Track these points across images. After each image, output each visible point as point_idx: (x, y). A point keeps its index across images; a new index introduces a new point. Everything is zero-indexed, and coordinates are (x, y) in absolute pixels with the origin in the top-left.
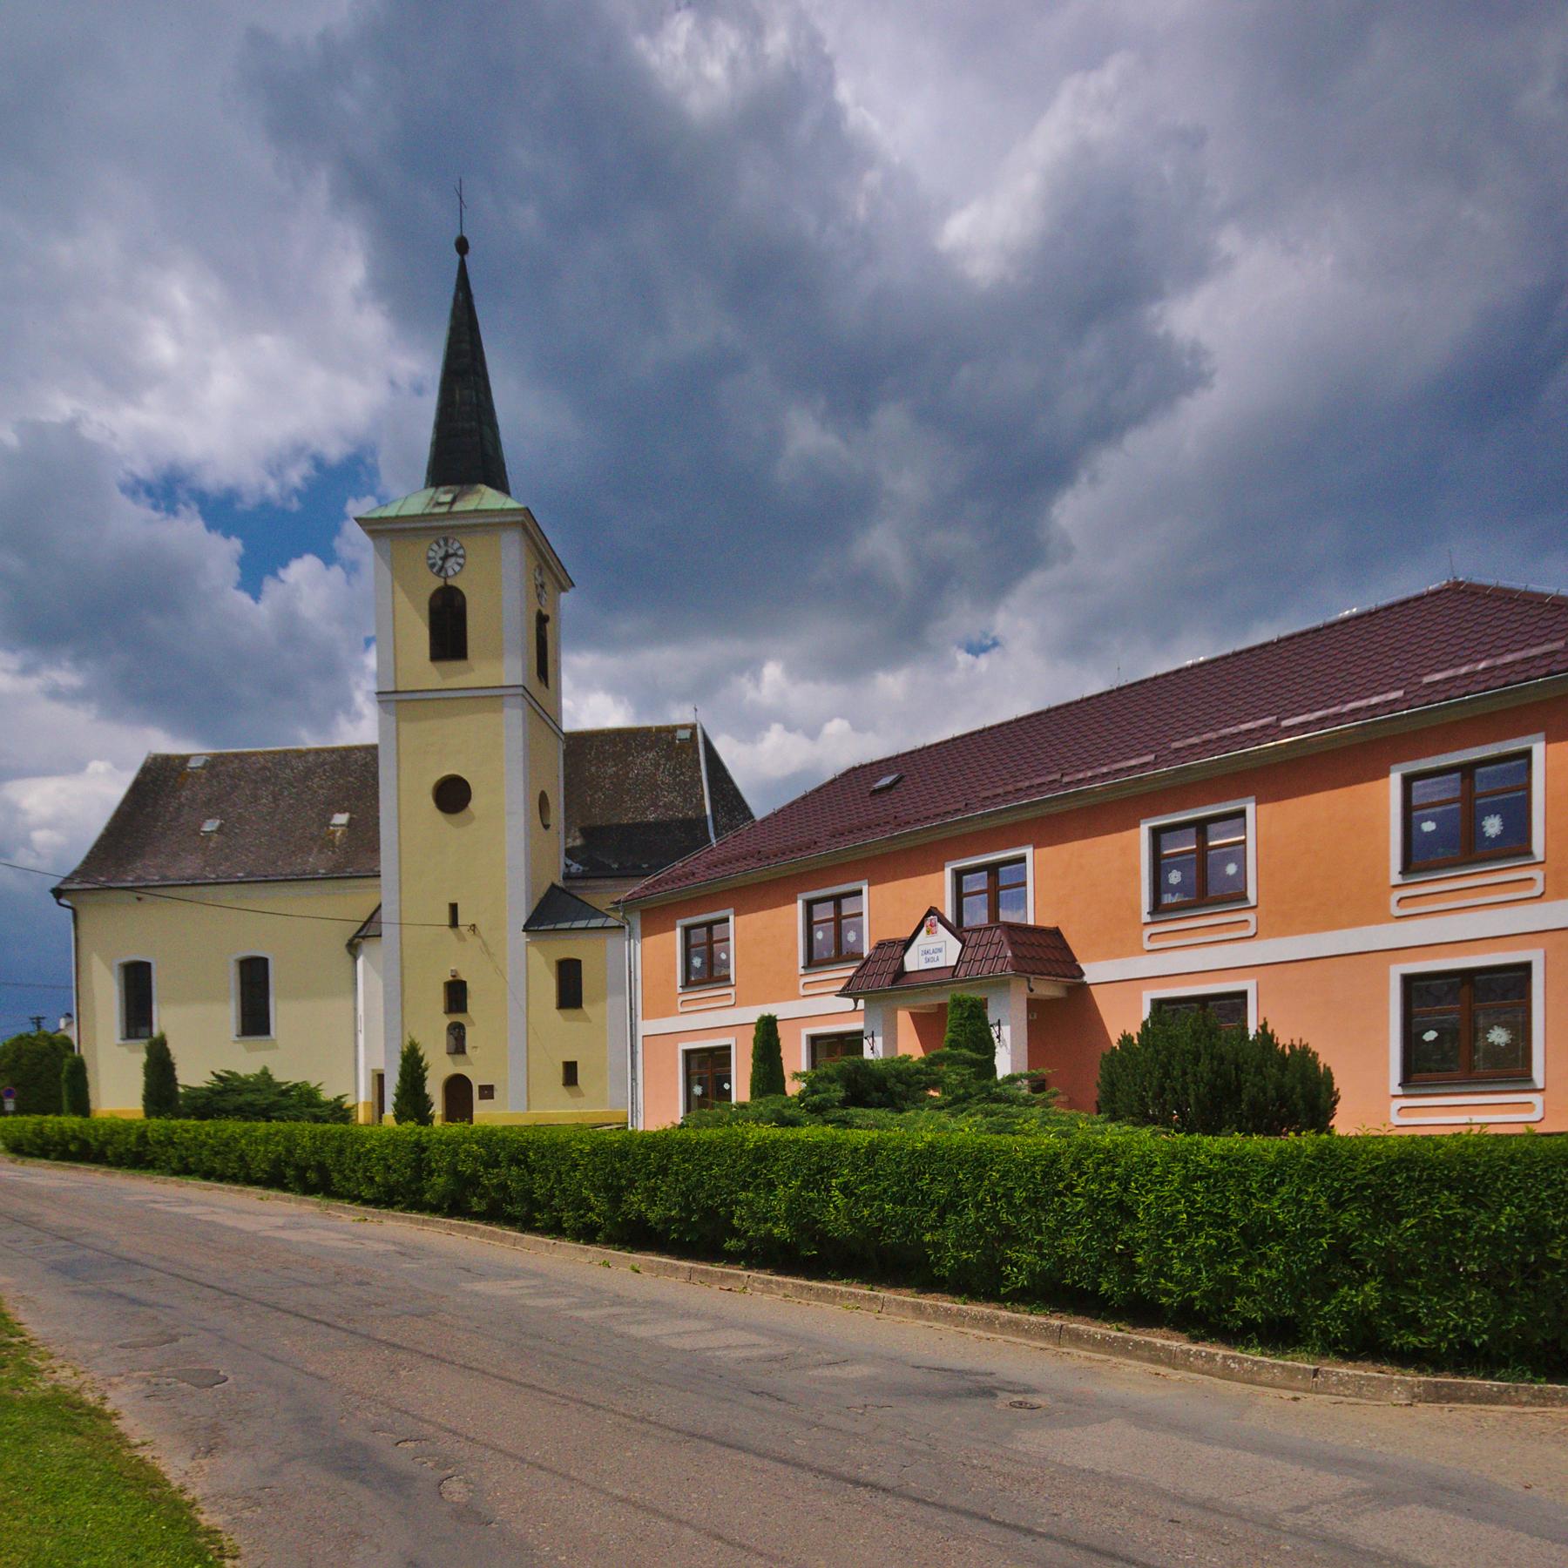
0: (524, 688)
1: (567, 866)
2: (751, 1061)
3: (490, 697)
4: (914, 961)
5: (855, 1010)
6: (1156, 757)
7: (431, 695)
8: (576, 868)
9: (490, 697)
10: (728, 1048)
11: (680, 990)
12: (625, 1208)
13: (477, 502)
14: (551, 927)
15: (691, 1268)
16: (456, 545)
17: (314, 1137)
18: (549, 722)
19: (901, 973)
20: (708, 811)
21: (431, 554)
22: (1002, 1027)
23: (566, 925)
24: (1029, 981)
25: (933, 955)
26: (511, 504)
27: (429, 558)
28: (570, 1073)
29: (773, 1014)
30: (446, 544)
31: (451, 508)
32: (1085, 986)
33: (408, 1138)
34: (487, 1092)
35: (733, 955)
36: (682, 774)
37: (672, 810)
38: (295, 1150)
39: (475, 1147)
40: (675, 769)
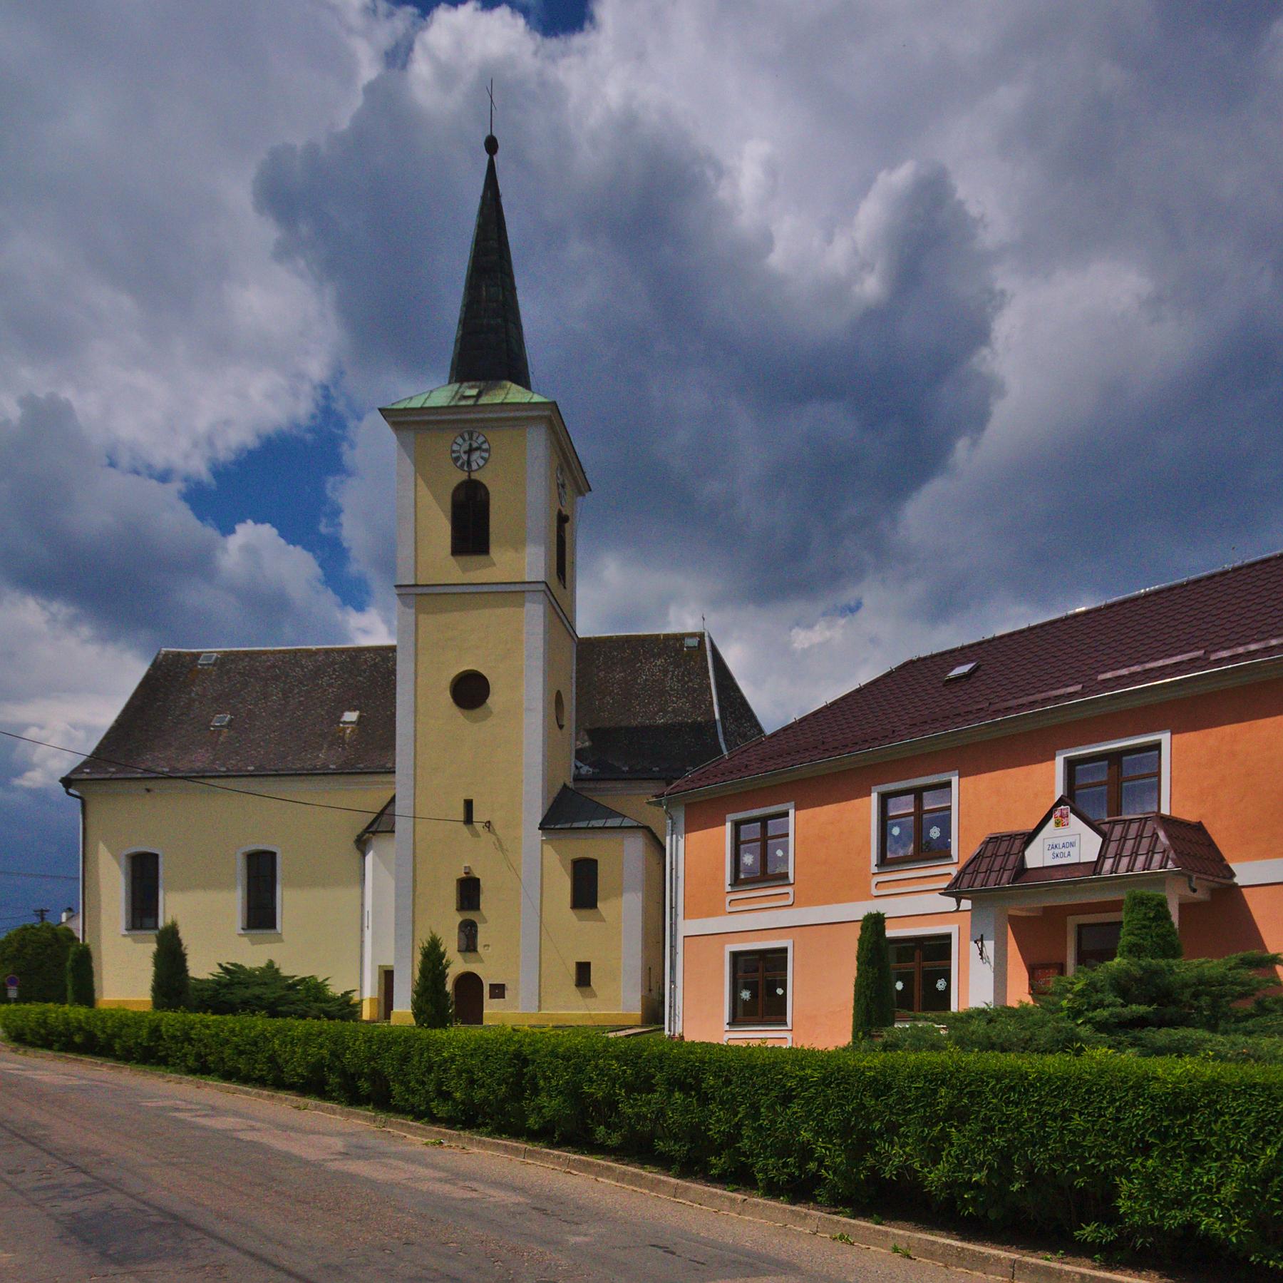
0: (546, 583)
1: (577, 767)
2: (856, 963)
3: (512, 593)
4: (1036, 856)
5: (957, 911)
6: (1083, 687)
7: (454, 590)
8: (585, 770)
9: (512, 593)
10: (785, 950)
11: (728, 889)
12: (870, 1160)
13: (504, 396)
14: (567, 825)
15: (1015, 1261)
16: (481, 439)
17: (370, 1040)
18: (566, 622)
19: (1021, 871)
20: (717, 716)
21: (456, 448)
22: (984, 942)
23: (583, 824)
24: (1190, 878)
25: (1063, 850)
26: (537, 398)
27: (453, 452)
28: (583, 974)
29: (882, 912)
30: (471, 438)
31: (477, 400)
32: (1237, 888)
33: (504, 1048)
34: (498, 991)
35: (791, 856)
36: (691, 680)
37: (681, 715)
38: (344, 1055)
39: (615, 1064)
40: (683, 675)
